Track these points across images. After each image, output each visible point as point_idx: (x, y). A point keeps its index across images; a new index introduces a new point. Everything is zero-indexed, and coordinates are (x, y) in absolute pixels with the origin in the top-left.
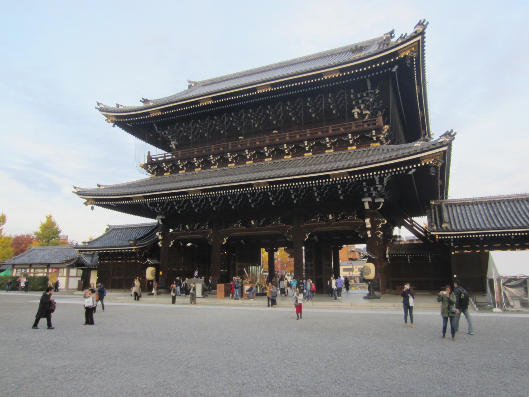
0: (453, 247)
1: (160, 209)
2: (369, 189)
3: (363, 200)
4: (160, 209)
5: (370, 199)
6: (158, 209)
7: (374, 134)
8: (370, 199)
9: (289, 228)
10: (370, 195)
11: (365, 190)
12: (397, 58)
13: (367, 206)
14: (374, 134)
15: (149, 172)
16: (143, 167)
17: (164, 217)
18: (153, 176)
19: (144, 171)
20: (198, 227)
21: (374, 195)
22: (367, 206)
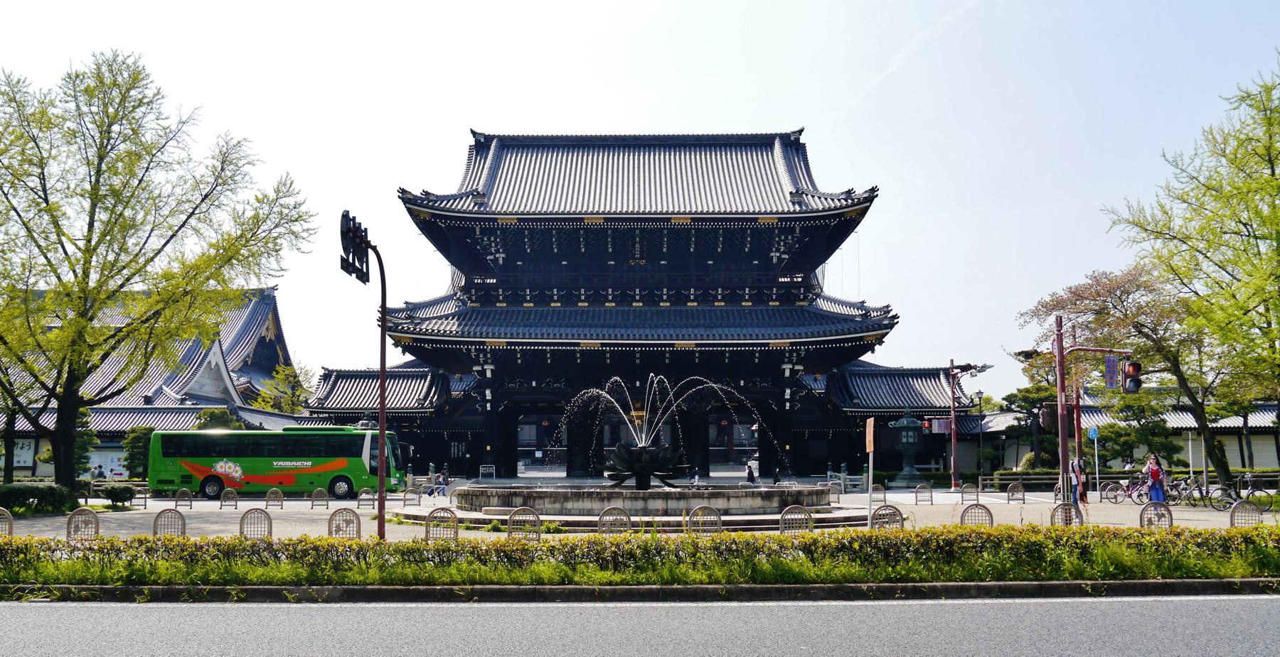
2: (791, 355)
3: (784, 366)
6: (485, 356)
10: (790, 362)
13: (787, 374)
17: (492, 367)
22: (787, 374)
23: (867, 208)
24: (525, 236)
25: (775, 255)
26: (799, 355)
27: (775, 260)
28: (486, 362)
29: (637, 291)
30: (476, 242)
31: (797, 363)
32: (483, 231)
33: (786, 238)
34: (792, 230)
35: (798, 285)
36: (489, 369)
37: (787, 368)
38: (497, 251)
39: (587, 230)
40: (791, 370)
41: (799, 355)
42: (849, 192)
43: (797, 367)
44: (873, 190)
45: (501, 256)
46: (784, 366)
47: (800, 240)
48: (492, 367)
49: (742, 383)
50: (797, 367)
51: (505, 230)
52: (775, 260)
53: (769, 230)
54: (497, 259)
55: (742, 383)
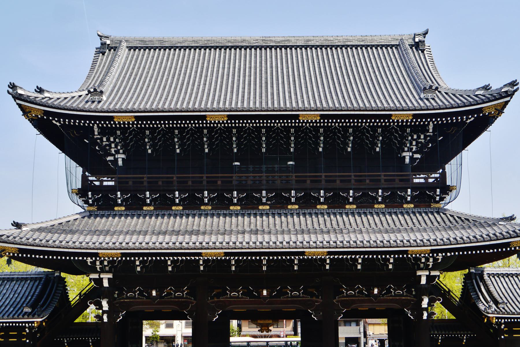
0: (503, 329)
1: (106, 263)
2: (427, 260)
3: (419, 273)
4: (106, 263)
5: (427, 273)
7: (438, 193)
8: (427, 273)
9: (317, 302)
11: (423, 260)
12: (481, 115)
13: (423, 281)
14: (438, 193)
15: (86, 202)
16: (77, 194)
17: (110, 276)
18: (92, 208)
19: (80, 202)
20: (169, 294)
21: (430, 267)
22: (423, 281)
23: (507, 103)
24: (144, 136)
25: (407, 155)
26: (435, 260)
27: (407, 160)
28: (103, 271)
29: (264, 193)
30: (94, 142)
31: (434, 268)
32: (103, 131)
33: (419, 137)
34: (424, 129)
35: (432, 187)
36: (106, 278)
37: (423, 275)
38: (117, 152)
39: (211, 130)
40: (429, 277)
41: (435, 260)
42: (486, 88)
43: (433, 273)
44: (513, 84)
45: (121, 157)
46: (419, 273)
47: (433, 140)
48: (110, 276)
49: (376, 291)
50: (433, 273)
51: (124, 129)
52: (407, 160)
53: (403, 127)
54: (116, 160)
55: (376, 291)
